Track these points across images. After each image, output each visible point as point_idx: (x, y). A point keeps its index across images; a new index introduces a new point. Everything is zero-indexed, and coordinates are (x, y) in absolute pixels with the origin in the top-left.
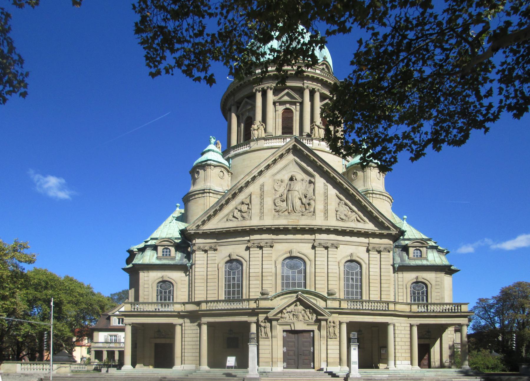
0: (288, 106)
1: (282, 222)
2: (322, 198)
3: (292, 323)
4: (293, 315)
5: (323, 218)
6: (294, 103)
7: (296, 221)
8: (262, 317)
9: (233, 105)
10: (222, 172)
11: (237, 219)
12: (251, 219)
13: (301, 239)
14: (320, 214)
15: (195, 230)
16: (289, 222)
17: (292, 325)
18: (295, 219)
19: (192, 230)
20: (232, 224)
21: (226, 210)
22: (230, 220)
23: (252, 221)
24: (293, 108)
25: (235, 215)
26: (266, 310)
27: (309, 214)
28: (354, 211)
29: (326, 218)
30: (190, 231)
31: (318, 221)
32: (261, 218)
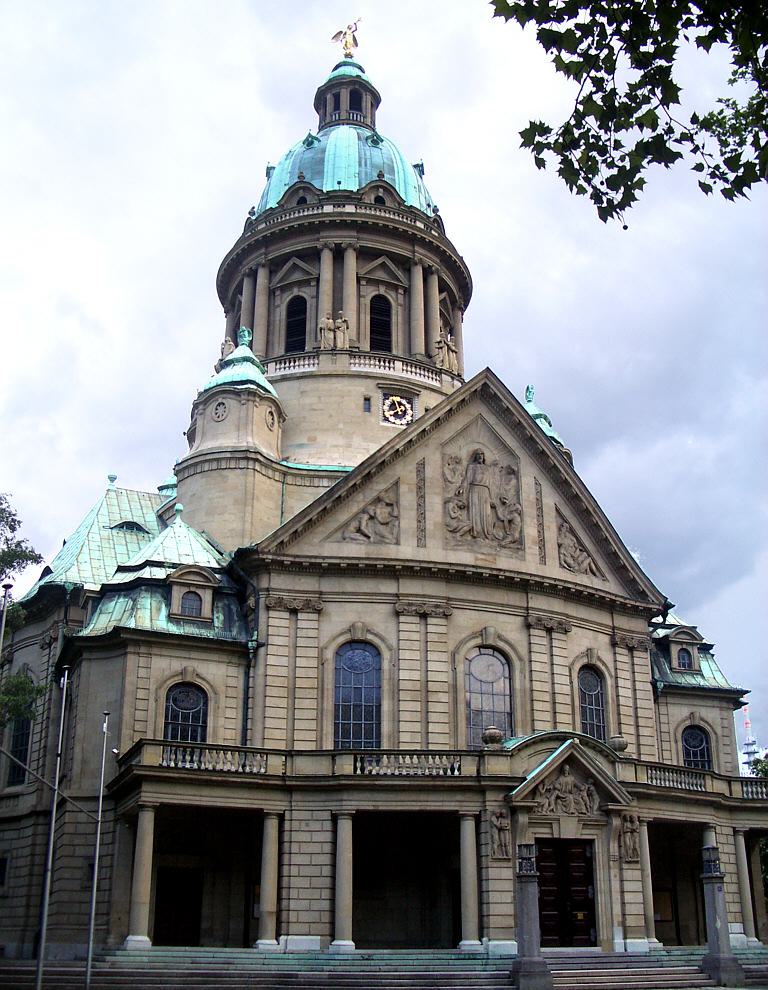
0: (382, 290)
1: (463, 557)
2: (534, 512)
3: (554, 819)
4: (558, 797)
5: (538, 558)
6: (395, 288)
7: (490, 558)
8: (493, 802)
9: (263, 266)
10: (272, 414)
11: (369, 537)
12: (398, 543)
13: (502, 605)
14: (532, 550)
15: (273, 554)
16: (477, 559)
17: (555, 826)
18: (489, 554)
19: (269, 553)
20: (354, 550)
21: (343, 516)
22: (352, 539)
23: (400, 547)
24: (391, 296)
25: (362, 528)
26: (505, 785)
27: (512, 545)
28: (584, 549)
29: (543, 560)
30: (265, 557)
31: (529, 564)
32: (421, 541)
